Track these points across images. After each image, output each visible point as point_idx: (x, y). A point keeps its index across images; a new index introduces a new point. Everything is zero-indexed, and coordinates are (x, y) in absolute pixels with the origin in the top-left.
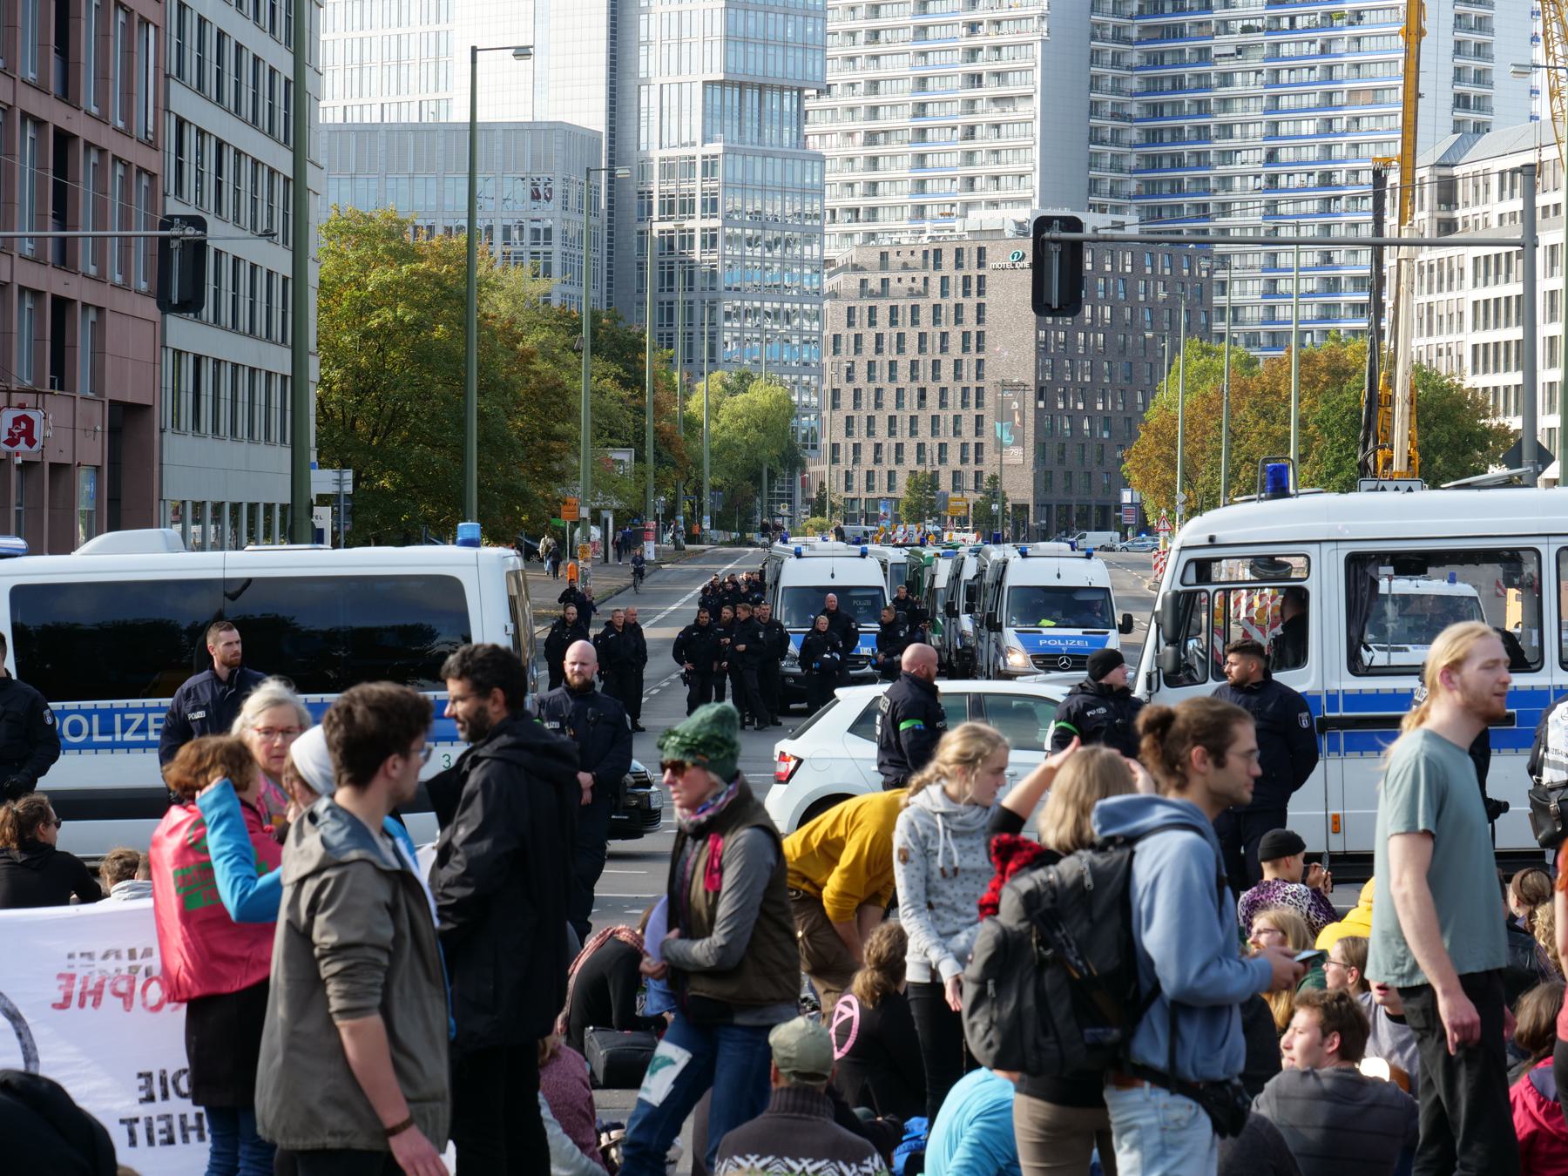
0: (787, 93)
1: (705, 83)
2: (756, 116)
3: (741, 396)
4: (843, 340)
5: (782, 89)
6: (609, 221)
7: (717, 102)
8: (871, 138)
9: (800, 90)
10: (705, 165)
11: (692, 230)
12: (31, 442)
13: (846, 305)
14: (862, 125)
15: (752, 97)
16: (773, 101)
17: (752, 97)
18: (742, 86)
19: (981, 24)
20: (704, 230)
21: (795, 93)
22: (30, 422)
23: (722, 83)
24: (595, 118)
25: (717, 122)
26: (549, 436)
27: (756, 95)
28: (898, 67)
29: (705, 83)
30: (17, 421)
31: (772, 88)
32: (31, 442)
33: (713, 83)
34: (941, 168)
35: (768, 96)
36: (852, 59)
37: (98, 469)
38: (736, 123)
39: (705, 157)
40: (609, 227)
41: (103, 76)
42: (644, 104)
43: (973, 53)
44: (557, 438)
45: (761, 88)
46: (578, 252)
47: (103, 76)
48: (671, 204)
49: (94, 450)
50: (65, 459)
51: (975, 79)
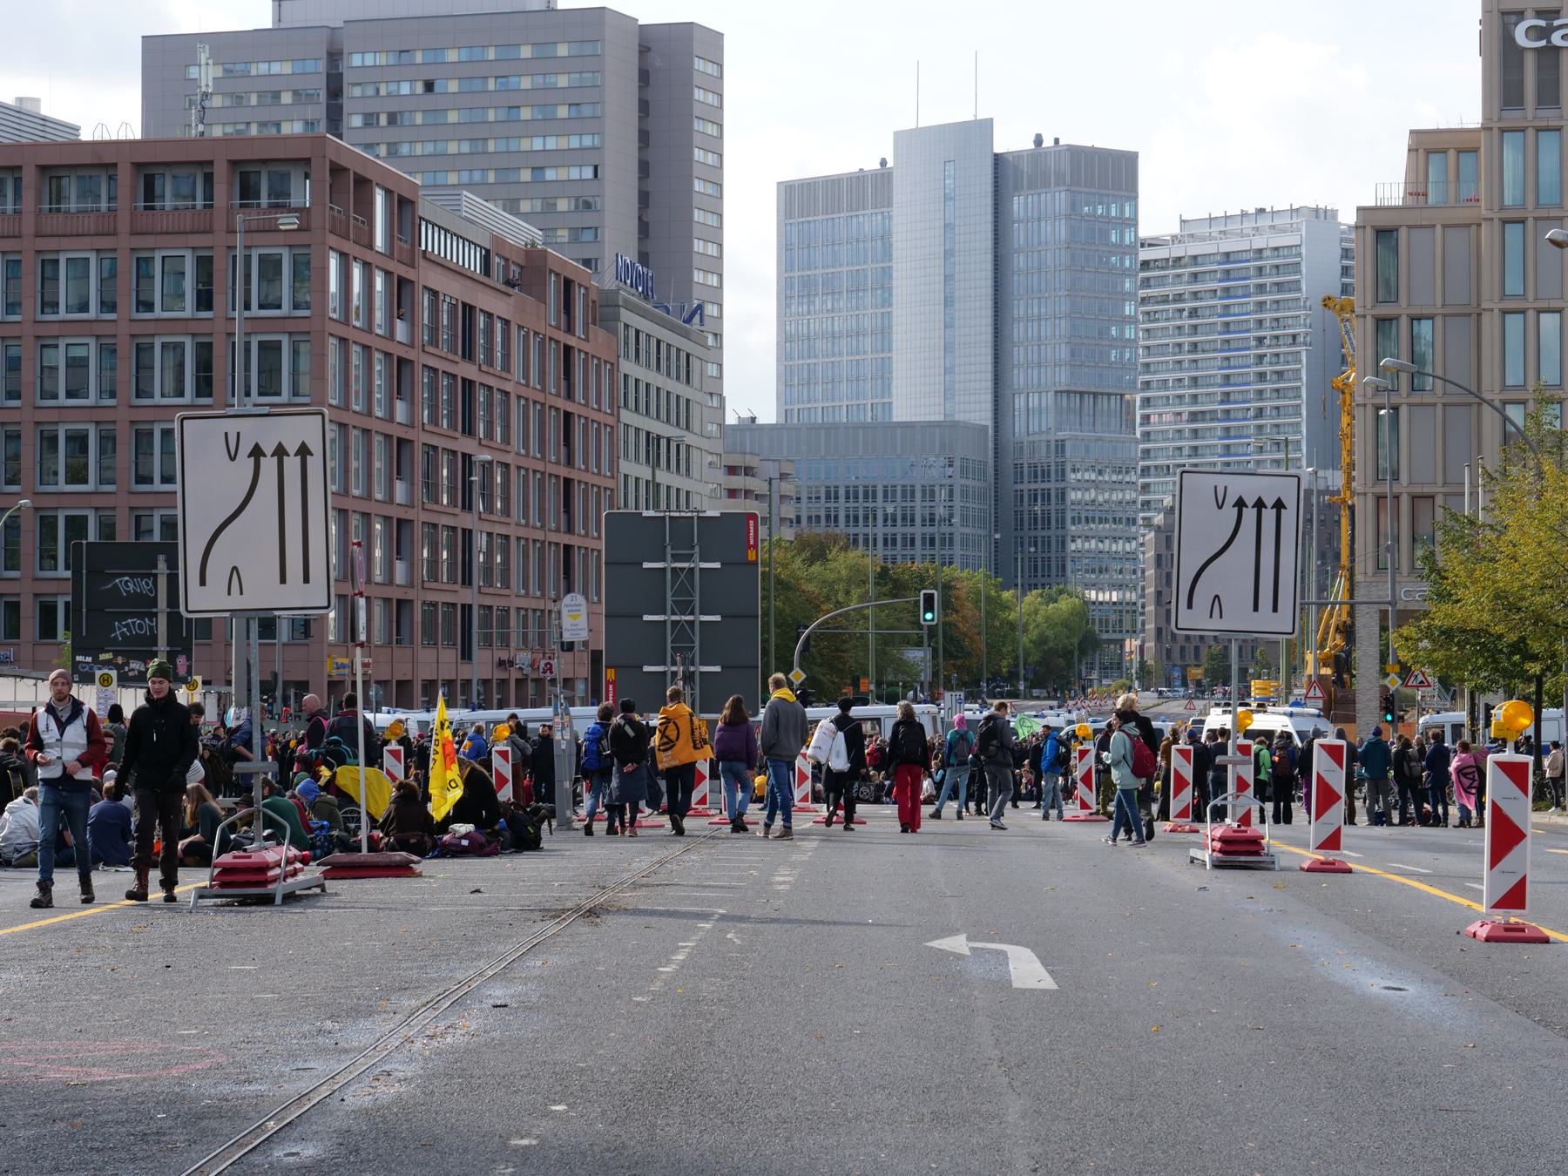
0: (1113, 397)
1: (1056, 392)
2: (1091, 413)
3: (1051, 606)
4: (1164, 558)
5: (1109, 395)
6: (996, 483)
7: (1065, 405)
8: (1194, 417)
9: (1122, 396)
10: (1057, 446)
11: (1049, 490)
12: (551, 672)
13: (1165, 534)
14: (1187, 409)
15: (1089, 401)
16: (1103, 403)
17: (1089, 401)
18: (1082, 394)
19: (1265, 338)
20: (1057, 489)
21: (1119, 397)
22: (551, 665)
23: (1068, 392)
24: (981, 414)
25: (1064, 417)
26: (837, 650)
27: (1091, 400)
28: (1212, 370)
29: (1056, 392)
30: (546, 664)
31: (1102, 394)
32: (551, 672)
33: (1061, 392)
34: (1241, 437)
35: (1100, 400)
36: (1180, 362)
37: (586, 679)
38: (1078, 417)
39: (1057, 441)
40: (996, 488)
41: (586, 517)
42: (1017, 406)
43: (1261, 357)
44: (843, 651)
45: (1095, 395)
46: (972, 506)
47: (586, 517)
48: (1036, 472)
49: (584, 671)
50: (570, 676)
51: (1262, 376)
